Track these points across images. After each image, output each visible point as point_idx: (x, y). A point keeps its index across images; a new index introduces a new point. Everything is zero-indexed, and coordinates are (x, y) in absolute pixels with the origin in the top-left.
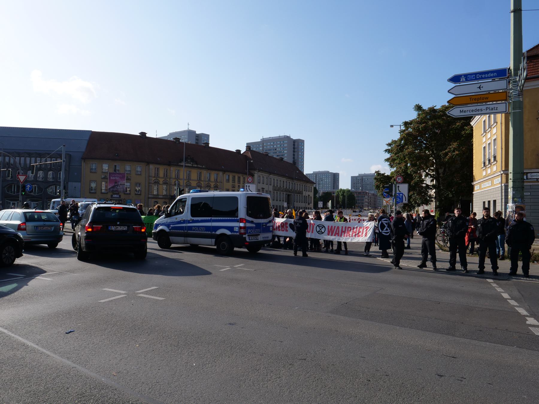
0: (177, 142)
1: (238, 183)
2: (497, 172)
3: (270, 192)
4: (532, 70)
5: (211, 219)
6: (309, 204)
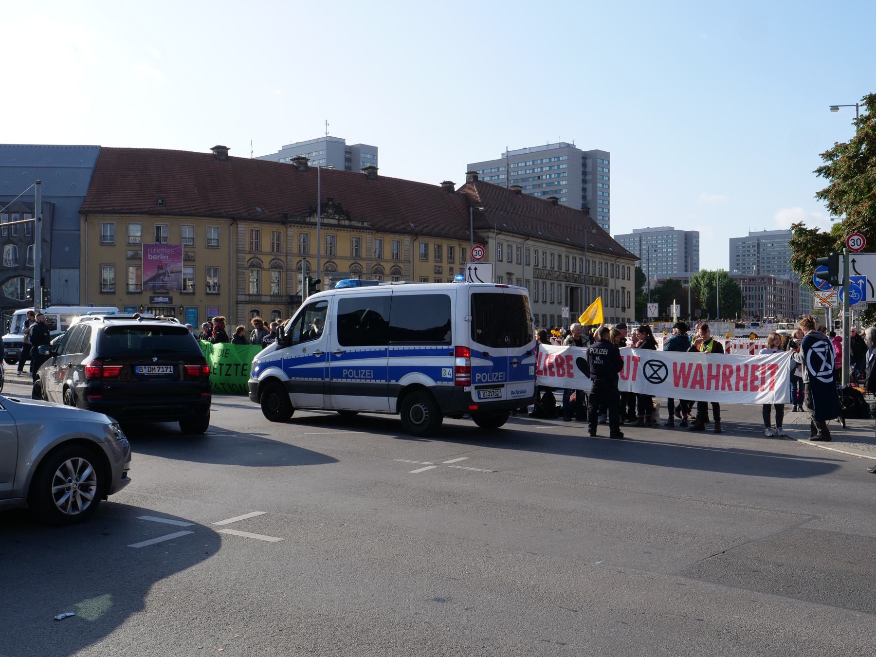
0: (302, 168)
1: (450, 263)
3: (528, 281)
5: (386, 349)
6: (624, 309)
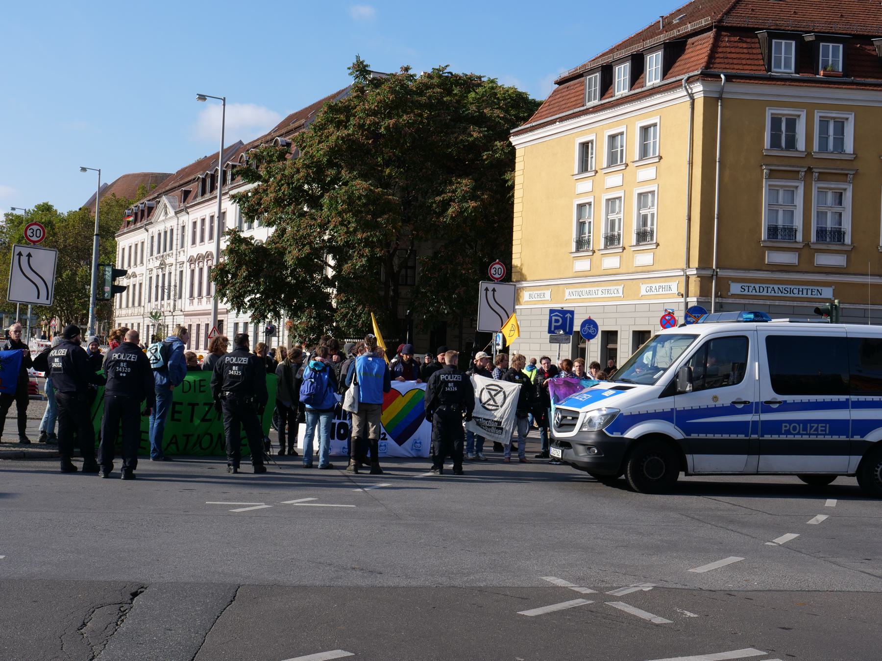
2: (653, 268)
4: (738, 53)
5: (847, 400)
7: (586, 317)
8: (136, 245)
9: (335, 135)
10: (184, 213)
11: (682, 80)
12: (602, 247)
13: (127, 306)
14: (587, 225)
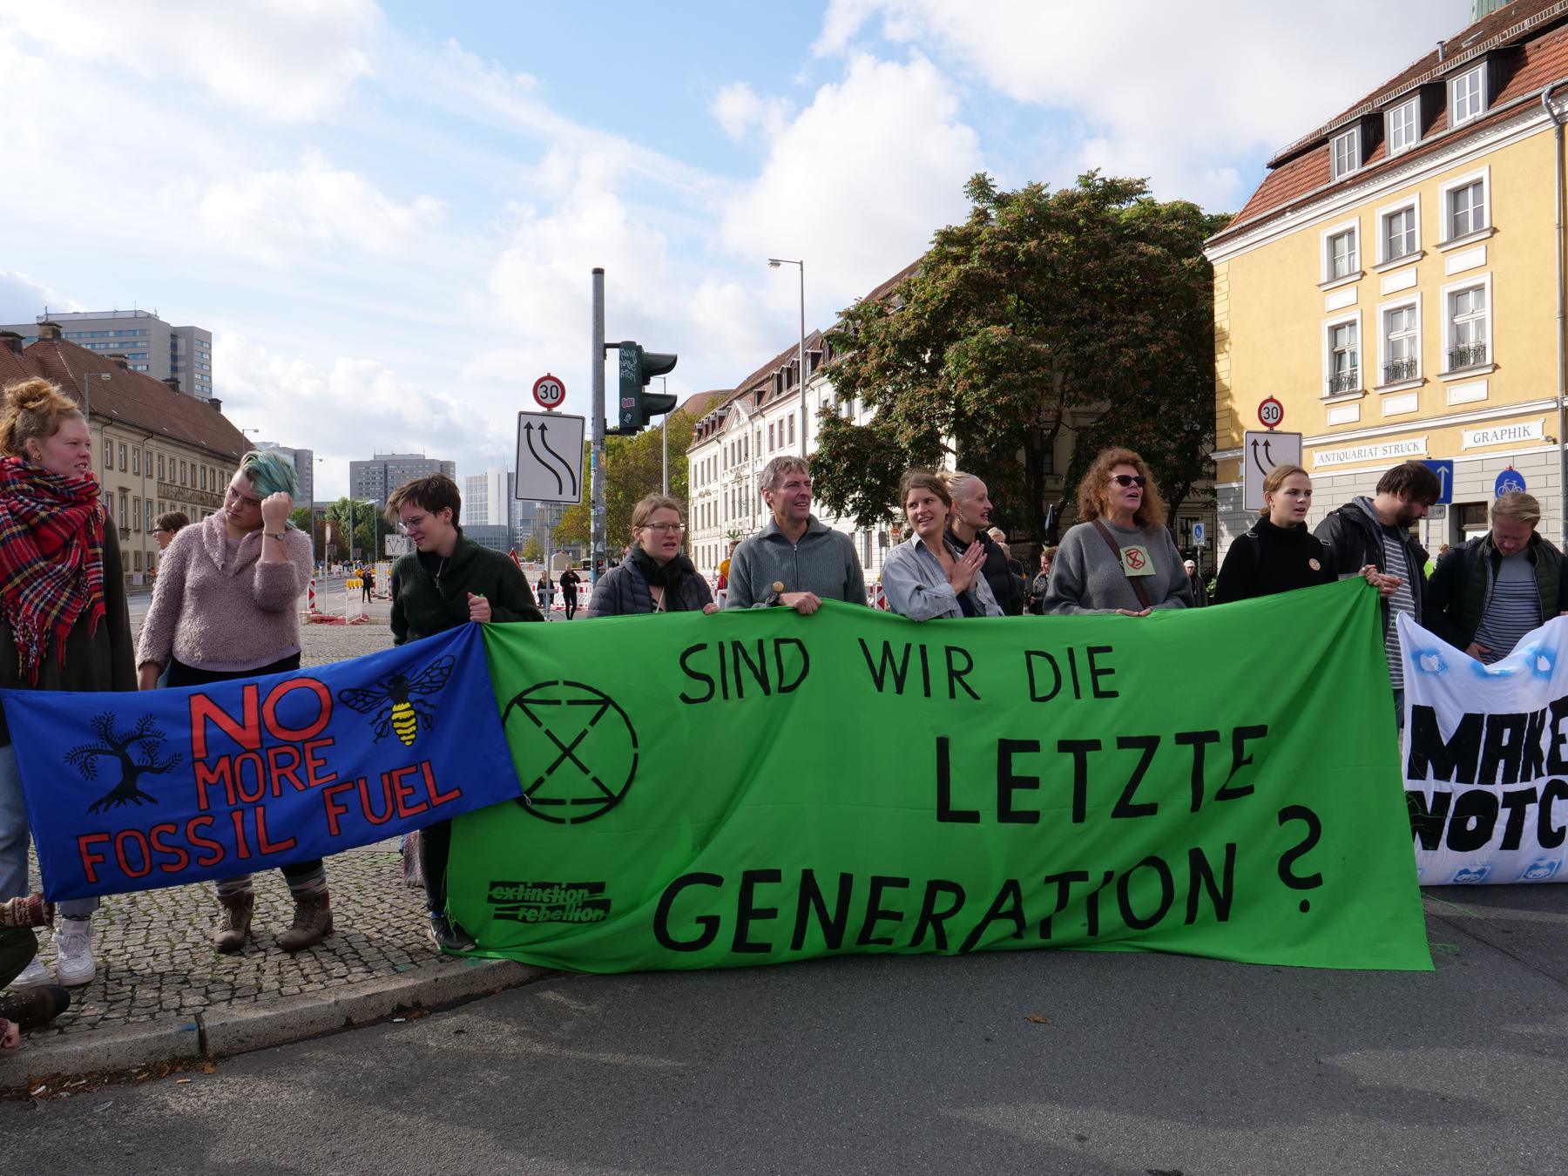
2: (1488, 404)
3: (150, 502)
7: (1504, 467)
8: (709, 460)
9: (954, 272)
10: (759, 416)
11: (1540, 95)
12: (1382, 383)
13: (703, 528)
14: (1347, 357)
